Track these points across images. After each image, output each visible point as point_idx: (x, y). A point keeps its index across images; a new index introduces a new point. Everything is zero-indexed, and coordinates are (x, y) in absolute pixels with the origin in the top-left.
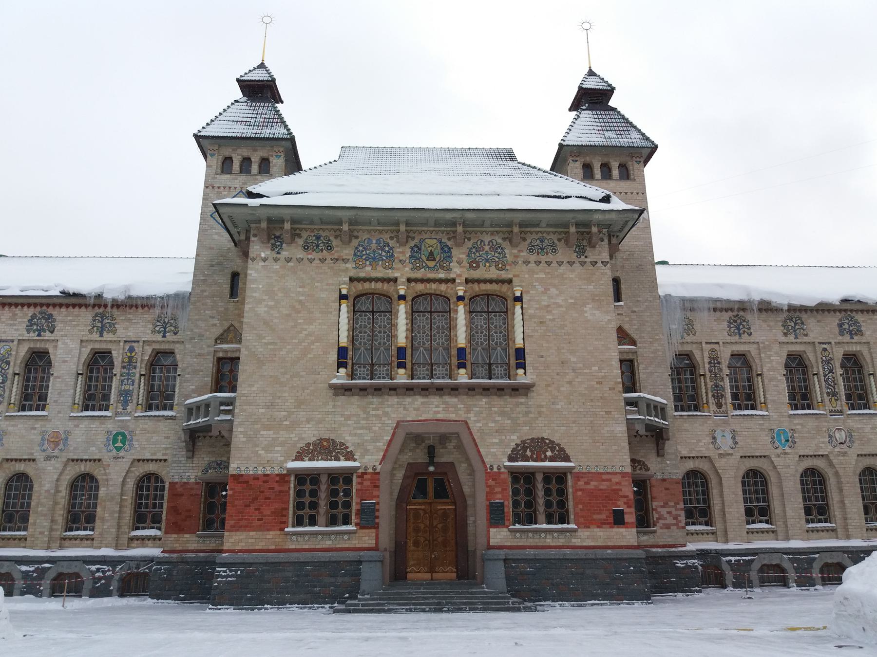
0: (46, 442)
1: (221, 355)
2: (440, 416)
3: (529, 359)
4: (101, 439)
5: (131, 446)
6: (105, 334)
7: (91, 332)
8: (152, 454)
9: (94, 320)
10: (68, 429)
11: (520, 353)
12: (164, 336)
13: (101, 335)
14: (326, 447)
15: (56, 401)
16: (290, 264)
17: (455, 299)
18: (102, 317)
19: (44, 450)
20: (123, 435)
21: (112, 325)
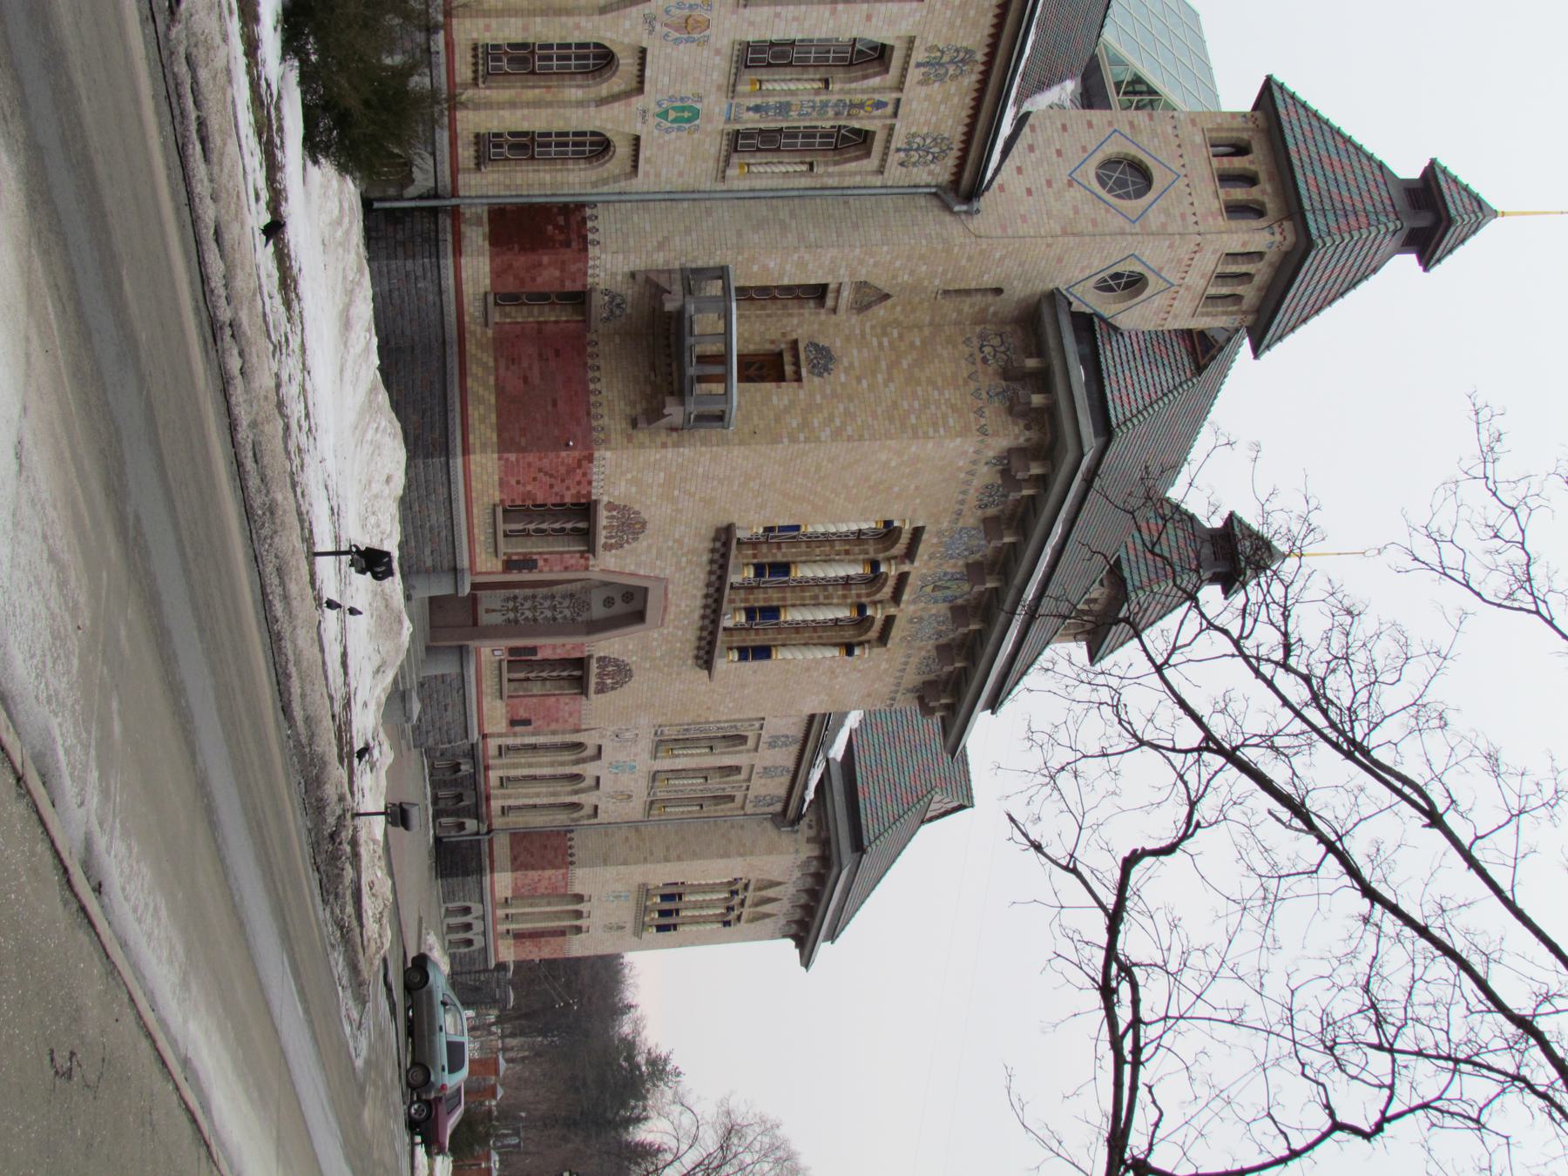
0: (686, 12)
1: (832, 286)
2: (672, 609)
3: (751, 665)
4: (687, 90)
5: (667, 131)
6: (923, 70)
7: (934, 48)
8: (648, 160)
9: (957, 50)
10: (712, 40)
11: (763, 652)
12: (898, 150)
13: (918, 65)
14: (631, 525)
15: (778, 15)
16: (962, 475)
17: (864, 600)
18: (962, 61)
19: (667, 12)
20: (689, 120)
21: (941, 79)
